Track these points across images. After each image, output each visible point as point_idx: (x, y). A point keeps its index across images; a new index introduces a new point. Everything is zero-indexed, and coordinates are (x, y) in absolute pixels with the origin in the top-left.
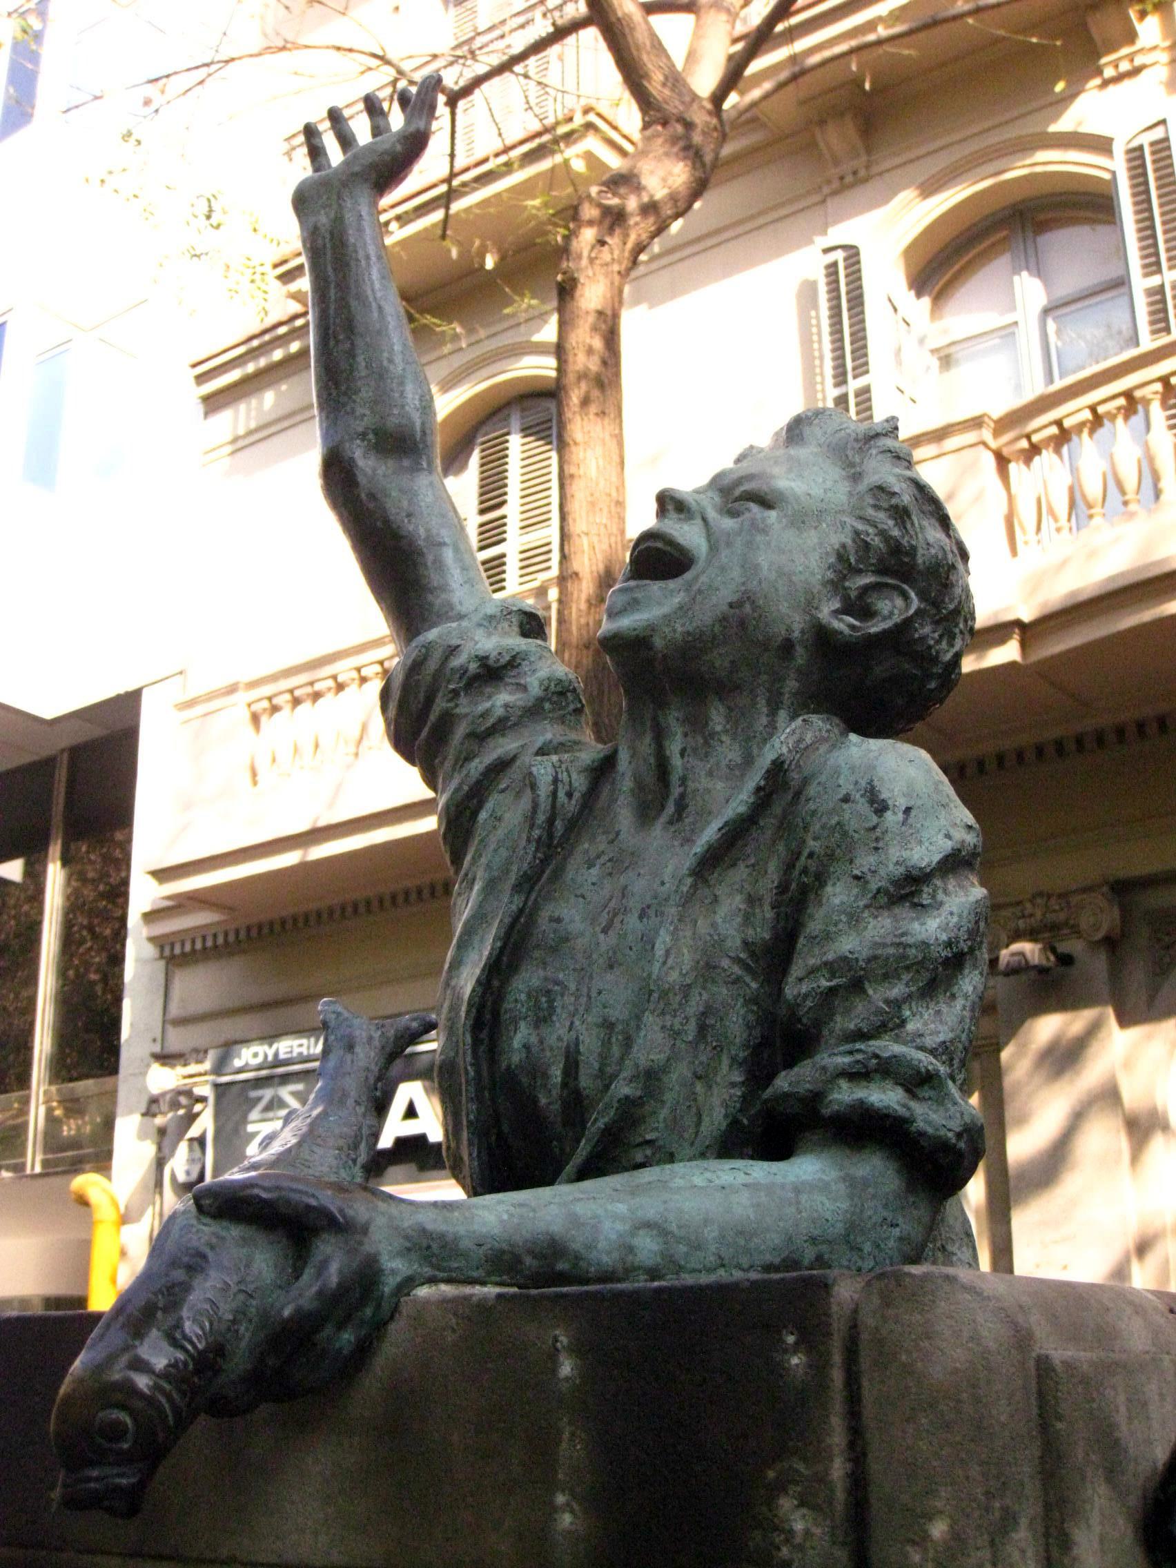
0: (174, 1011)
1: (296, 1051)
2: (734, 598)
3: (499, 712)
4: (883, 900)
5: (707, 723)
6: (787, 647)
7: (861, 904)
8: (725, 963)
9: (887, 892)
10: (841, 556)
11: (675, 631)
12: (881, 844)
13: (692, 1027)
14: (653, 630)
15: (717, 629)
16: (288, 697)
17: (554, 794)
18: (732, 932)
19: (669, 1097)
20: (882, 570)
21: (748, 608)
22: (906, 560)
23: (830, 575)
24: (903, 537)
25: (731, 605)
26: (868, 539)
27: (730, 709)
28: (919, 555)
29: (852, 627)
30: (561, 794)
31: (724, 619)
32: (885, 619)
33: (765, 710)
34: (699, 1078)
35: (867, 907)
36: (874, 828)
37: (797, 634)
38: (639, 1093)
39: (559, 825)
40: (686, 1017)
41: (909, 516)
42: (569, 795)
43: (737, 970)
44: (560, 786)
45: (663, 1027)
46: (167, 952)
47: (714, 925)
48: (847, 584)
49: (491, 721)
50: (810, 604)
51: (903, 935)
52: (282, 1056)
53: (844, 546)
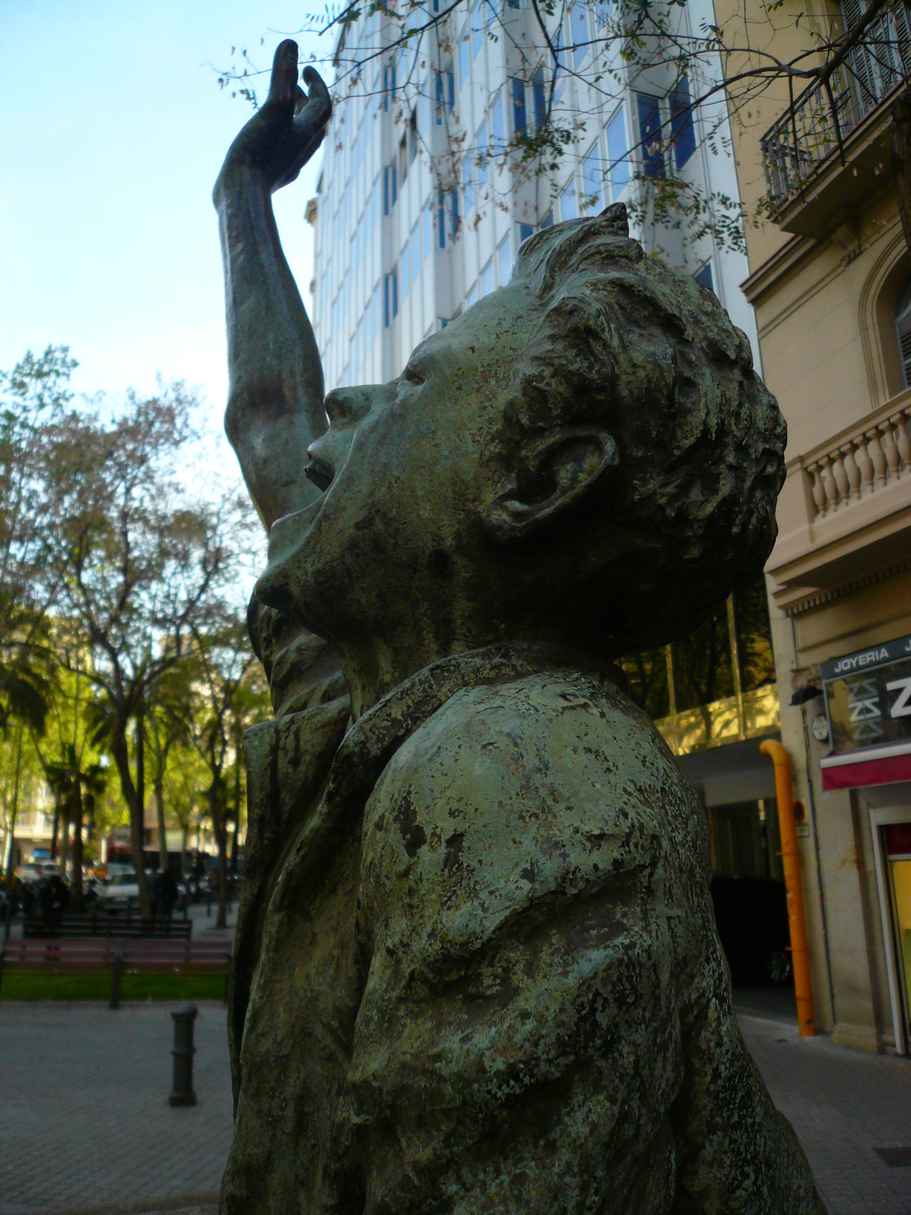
0: (800, 644)
1: (868, 659)
2: (362, 514)
3: (292, 657)
4: (422, 991)
5: (378, 673)
6: (440, 562)
7: (394, 995)
8: (319, 1031)
9: (425, 981)
10: (509, 417)
11: (306, 573)
12: (415, 901)
13: (290, 1112)
14: (286, 577)
15: (348, 560)
16: (826, 459)
17: (273, 765)
18: (324, 988)
19: (272, 1202)
20: (574, 420)
21: (379, 525)
22: (601, 397)
23: (495, 448)
24: (591, 367)
25: (358, 526)
26: (542, 386)
27: (396, 652)
28: (622, 384)
29: (517, 515)
30: (283, 765)
31: (353, 545)
32: (564, 491)
33: (434, 646)
34: (302, 1184)
35: (401, 1000)
36: (406, 874)
37: (449, 542)
38: (245, 1193)
39: (285, 796)
40: (285, 1100)
41: (597, 336)
42: (295, 762)
43: (329, 1040)
44: (281, 754)
45: (259, 1112)
46: (790, 613)
47: (308, 977)
48: (524, 453)
49: (287, 667)
50: (462, 495)
51: (438, 1057)
52: (861, 663)
53: (511, 404)
